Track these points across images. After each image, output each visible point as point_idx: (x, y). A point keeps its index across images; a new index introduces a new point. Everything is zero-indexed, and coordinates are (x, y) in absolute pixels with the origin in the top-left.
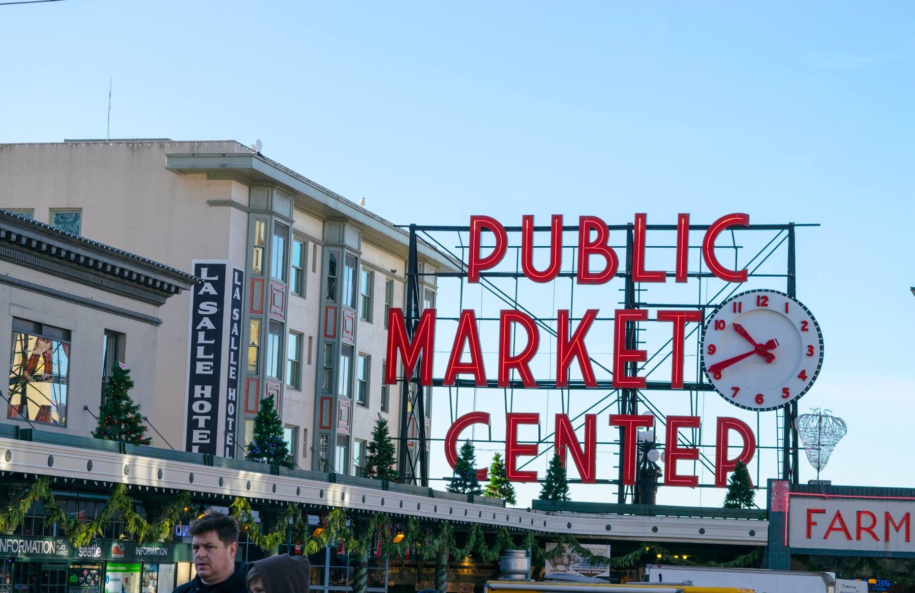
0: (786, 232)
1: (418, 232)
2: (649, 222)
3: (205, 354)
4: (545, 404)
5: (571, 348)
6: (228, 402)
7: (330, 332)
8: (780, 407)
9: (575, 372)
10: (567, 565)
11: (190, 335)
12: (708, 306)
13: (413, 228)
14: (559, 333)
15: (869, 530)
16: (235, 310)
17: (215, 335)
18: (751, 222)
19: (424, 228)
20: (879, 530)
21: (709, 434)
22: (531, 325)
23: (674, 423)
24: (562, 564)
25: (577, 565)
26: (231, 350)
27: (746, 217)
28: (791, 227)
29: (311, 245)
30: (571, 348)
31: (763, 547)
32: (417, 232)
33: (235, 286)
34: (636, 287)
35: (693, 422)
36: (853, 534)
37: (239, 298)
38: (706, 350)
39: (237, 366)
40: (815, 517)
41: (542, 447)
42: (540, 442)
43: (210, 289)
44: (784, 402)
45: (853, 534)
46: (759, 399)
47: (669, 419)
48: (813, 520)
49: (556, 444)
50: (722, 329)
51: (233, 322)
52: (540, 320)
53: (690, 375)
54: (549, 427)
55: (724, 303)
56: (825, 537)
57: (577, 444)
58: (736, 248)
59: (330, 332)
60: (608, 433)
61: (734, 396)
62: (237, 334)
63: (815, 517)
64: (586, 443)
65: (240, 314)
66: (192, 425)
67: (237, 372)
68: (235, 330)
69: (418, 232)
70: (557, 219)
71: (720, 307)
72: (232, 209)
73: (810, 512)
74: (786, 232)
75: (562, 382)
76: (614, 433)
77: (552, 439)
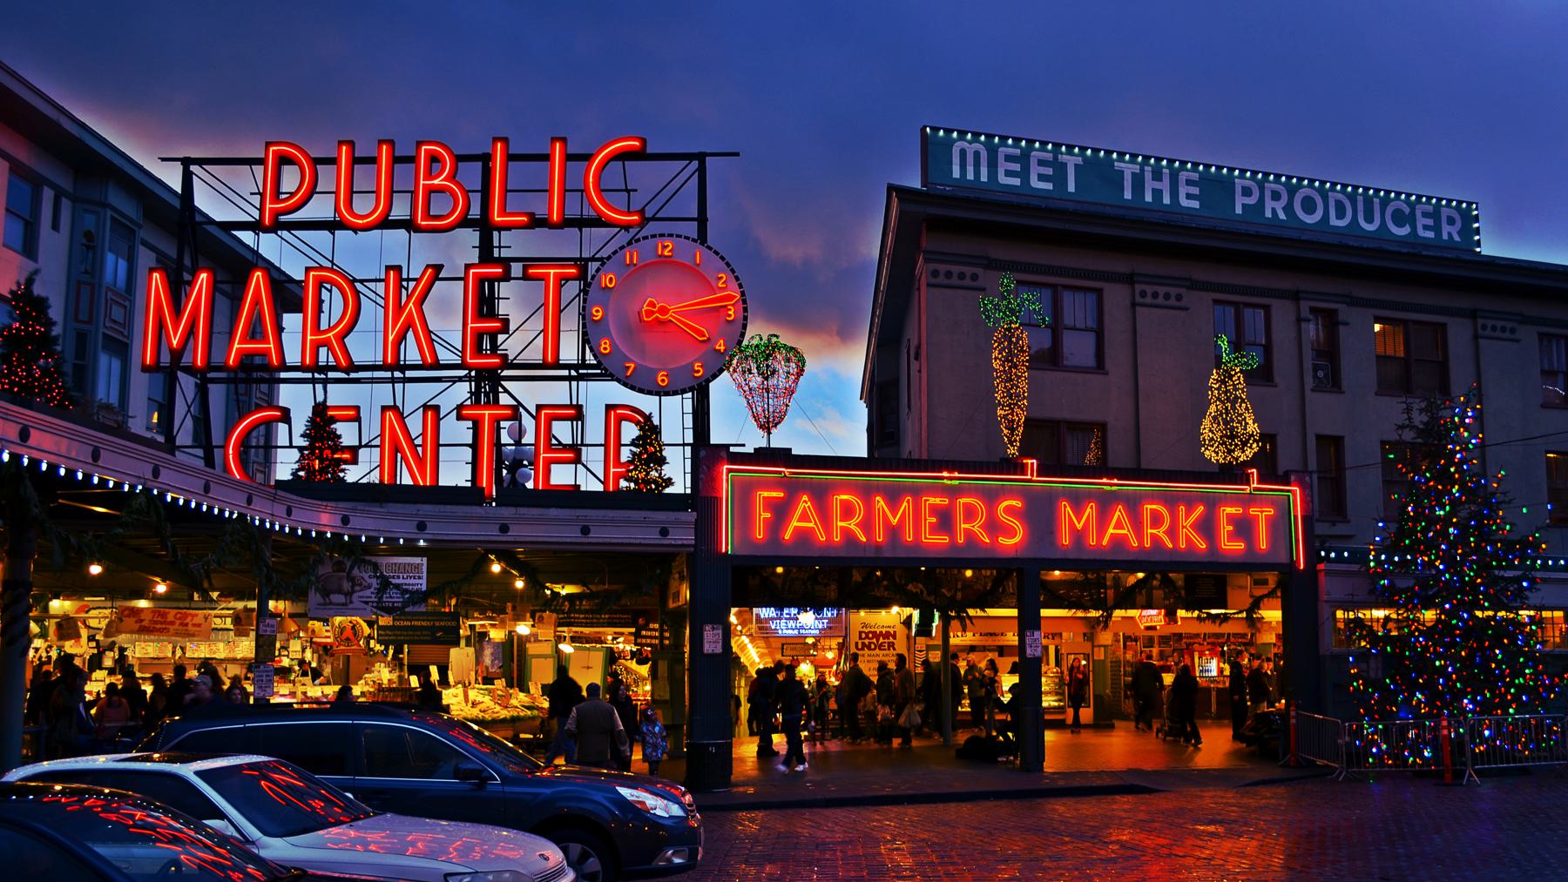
1: (194, 168)
4: (371, 397)
5: (406, 319)
7: (83, 316)
8: (691, 389)
9: (411, 353)
10: (349, 594)
12: (593, 259)
13: (186, 162)
14: (386, 299)
19: (201, 162)
21: (595, 429)
22: (352, 287)
23: (547, 414)
24: (340, 591)
25: (368, 593)
29: (48, 194)
30: (406, 319)
32: (192, 168)
34: (496, 243)
35: (576, 413)
41: (362, 452)
42: (360, 446)
47: (539, 407)
49: (382, 446)
52: (362, 281)
53: (569, 351)
54: (372, 428)
55: (615, 253)
57: (413, 447)
59: (83, 316)
60: (457, 431)
64: (424, 446)
69: (194, 168)
71: (609, 258)
75: (394, 368)
76: (463, 431)
77: (377, 442)
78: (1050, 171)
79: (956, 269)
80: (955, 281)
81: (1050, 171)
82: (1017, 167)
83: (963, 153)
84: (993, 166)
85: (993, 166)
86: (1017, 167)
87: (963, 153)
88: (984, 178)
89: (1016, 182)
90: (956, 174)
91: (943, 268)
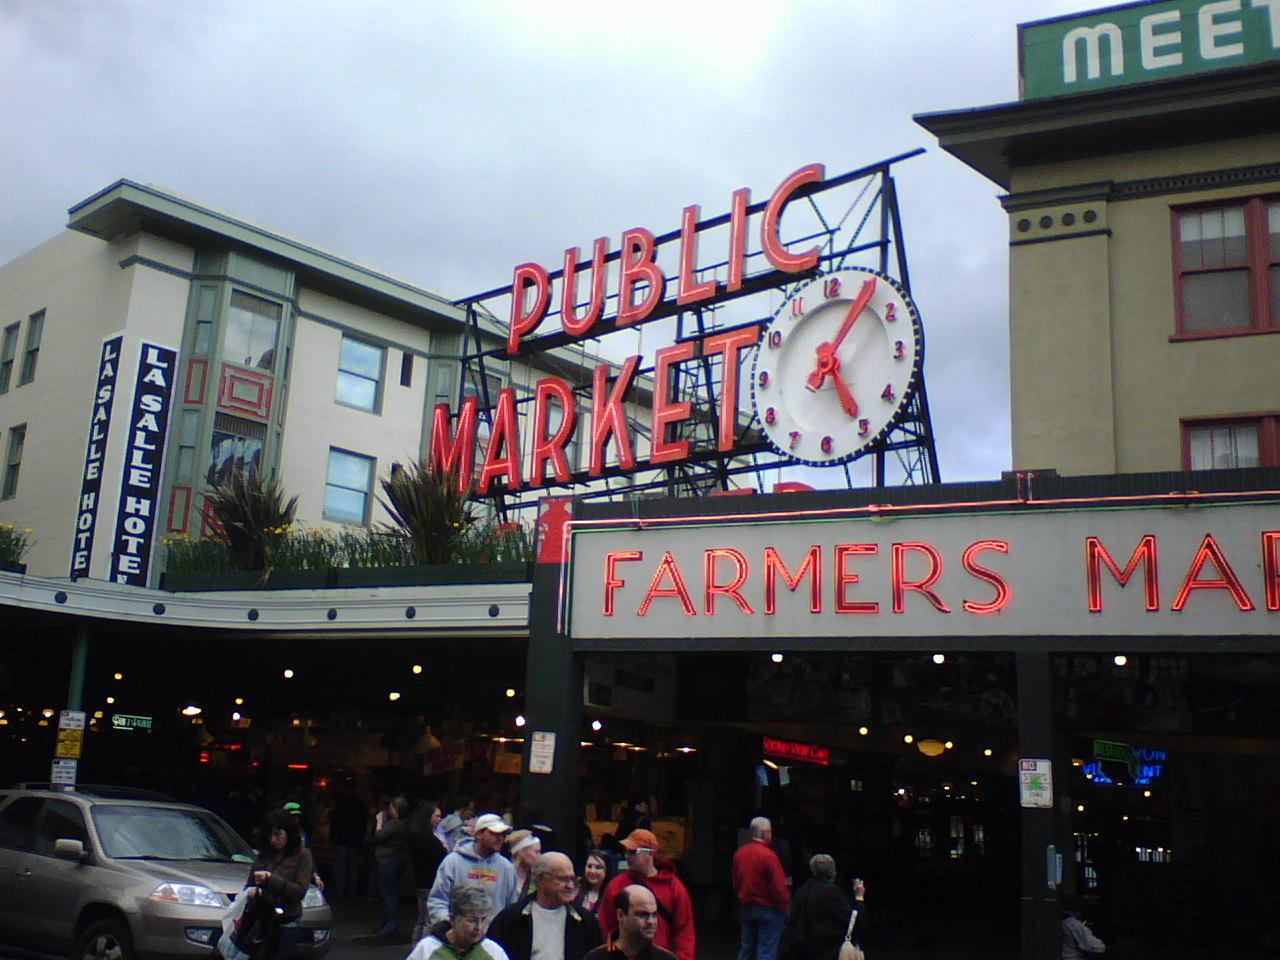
0: (880, 175)
1: (475, 306)
2: (704, 218)
3: (143, 462)
6: (123, 515)
11: (127, 437)
13: (469, 301)
15: (734, 592)
16: (147, 399)
17: (104, 426)
18: (829, 176)
19: (478, 298)
20: (754, 592)
26: (131, 447)
27: (821, 168)
28: (883, 167)
31: (524, 640)
33: (145, 368)
36: (697, 597)
37: (160, 381)
38: (757, 381)
39: (155, 472)
40: (622, 571)
43: (109, 371)
44: (860, 445)
45: (697, 597)
46: (827, 444)
48: (619, 576)
50: (777, 345)
51: (138, 413)
56: (643, 613)
58: (831, 232)
61: (792, 448)
62: (153, 427)
63: (622, 571)
65: (165, 404)
66: (77, 548)
67: (154, 480)
68: (149, 421)
69: (475, 306)
70: (602, 243)
72: (138, 266)
73: (613, 561)
74: (880, 175)
78: (1236, 27)
79: (1057, 212)
80: (1057, 229)
81: (1236, 27)
82: (1175, 38)
83: (1081, 45)
84: (1132, 46)
85: (1132, 46)
86: (1175, 38)
87: (1081, 45)
88: (1117, 67)
89: (1176, 59)
90: (1070, 75)
91: (1034, 215)
